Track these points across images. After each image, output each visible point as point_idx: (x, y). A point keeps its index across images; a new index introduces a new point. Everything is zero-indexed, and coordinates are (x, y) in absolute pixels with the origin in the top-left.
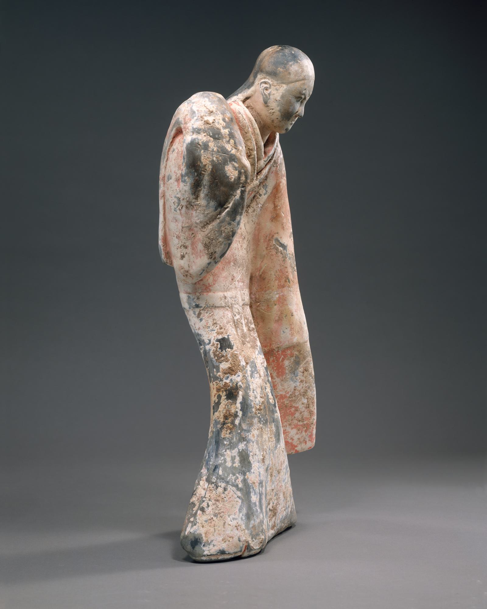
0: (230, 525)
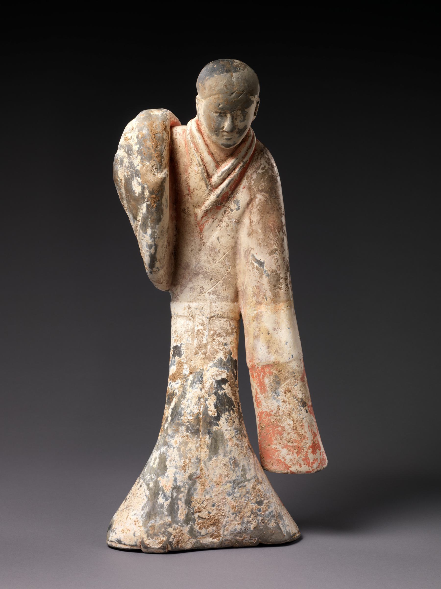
0: (130, 518)
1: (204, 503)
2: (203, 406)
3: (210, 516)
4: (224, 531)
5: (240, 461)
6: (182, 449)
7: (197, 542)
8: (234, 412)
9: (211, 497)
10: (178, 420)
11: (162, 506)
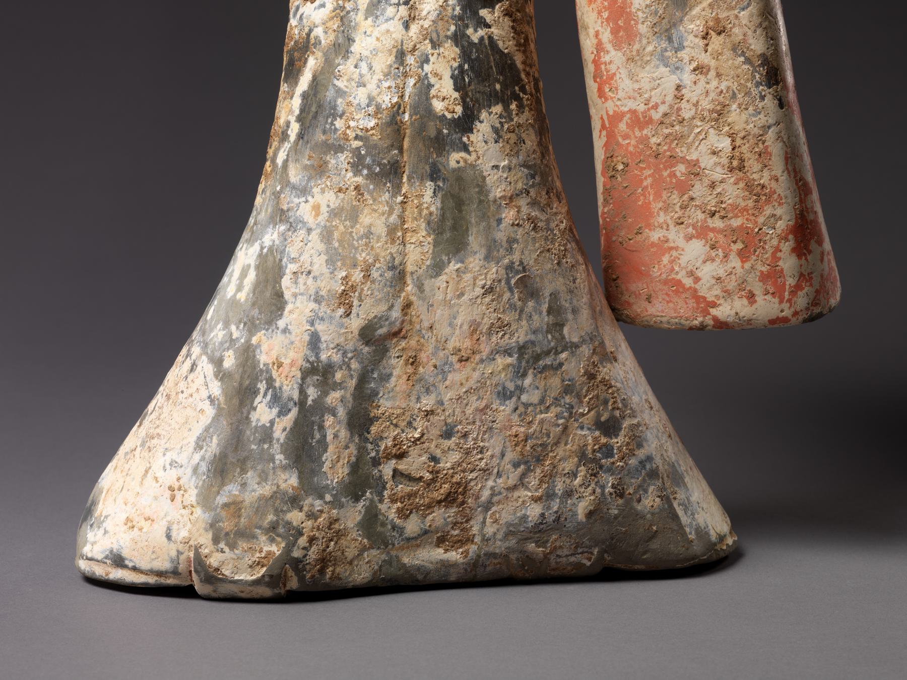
0: (156, 479)
1: (415, 424)
2: (411, 82)
3: (435, 472)
4: (484, 522)
5: (542, 277)
6: (336, 235)
7: (389, 562)
8: (521, 107)
9: (441, 403)
10: (324, 132)
11: (266, 434)
